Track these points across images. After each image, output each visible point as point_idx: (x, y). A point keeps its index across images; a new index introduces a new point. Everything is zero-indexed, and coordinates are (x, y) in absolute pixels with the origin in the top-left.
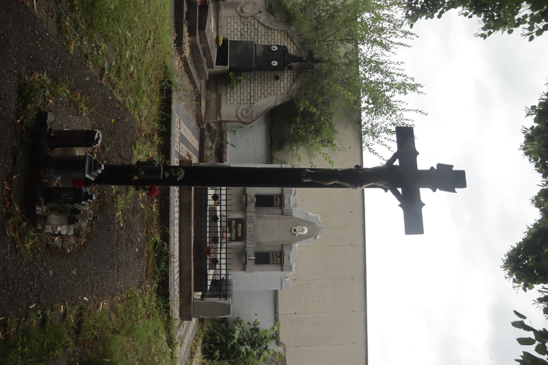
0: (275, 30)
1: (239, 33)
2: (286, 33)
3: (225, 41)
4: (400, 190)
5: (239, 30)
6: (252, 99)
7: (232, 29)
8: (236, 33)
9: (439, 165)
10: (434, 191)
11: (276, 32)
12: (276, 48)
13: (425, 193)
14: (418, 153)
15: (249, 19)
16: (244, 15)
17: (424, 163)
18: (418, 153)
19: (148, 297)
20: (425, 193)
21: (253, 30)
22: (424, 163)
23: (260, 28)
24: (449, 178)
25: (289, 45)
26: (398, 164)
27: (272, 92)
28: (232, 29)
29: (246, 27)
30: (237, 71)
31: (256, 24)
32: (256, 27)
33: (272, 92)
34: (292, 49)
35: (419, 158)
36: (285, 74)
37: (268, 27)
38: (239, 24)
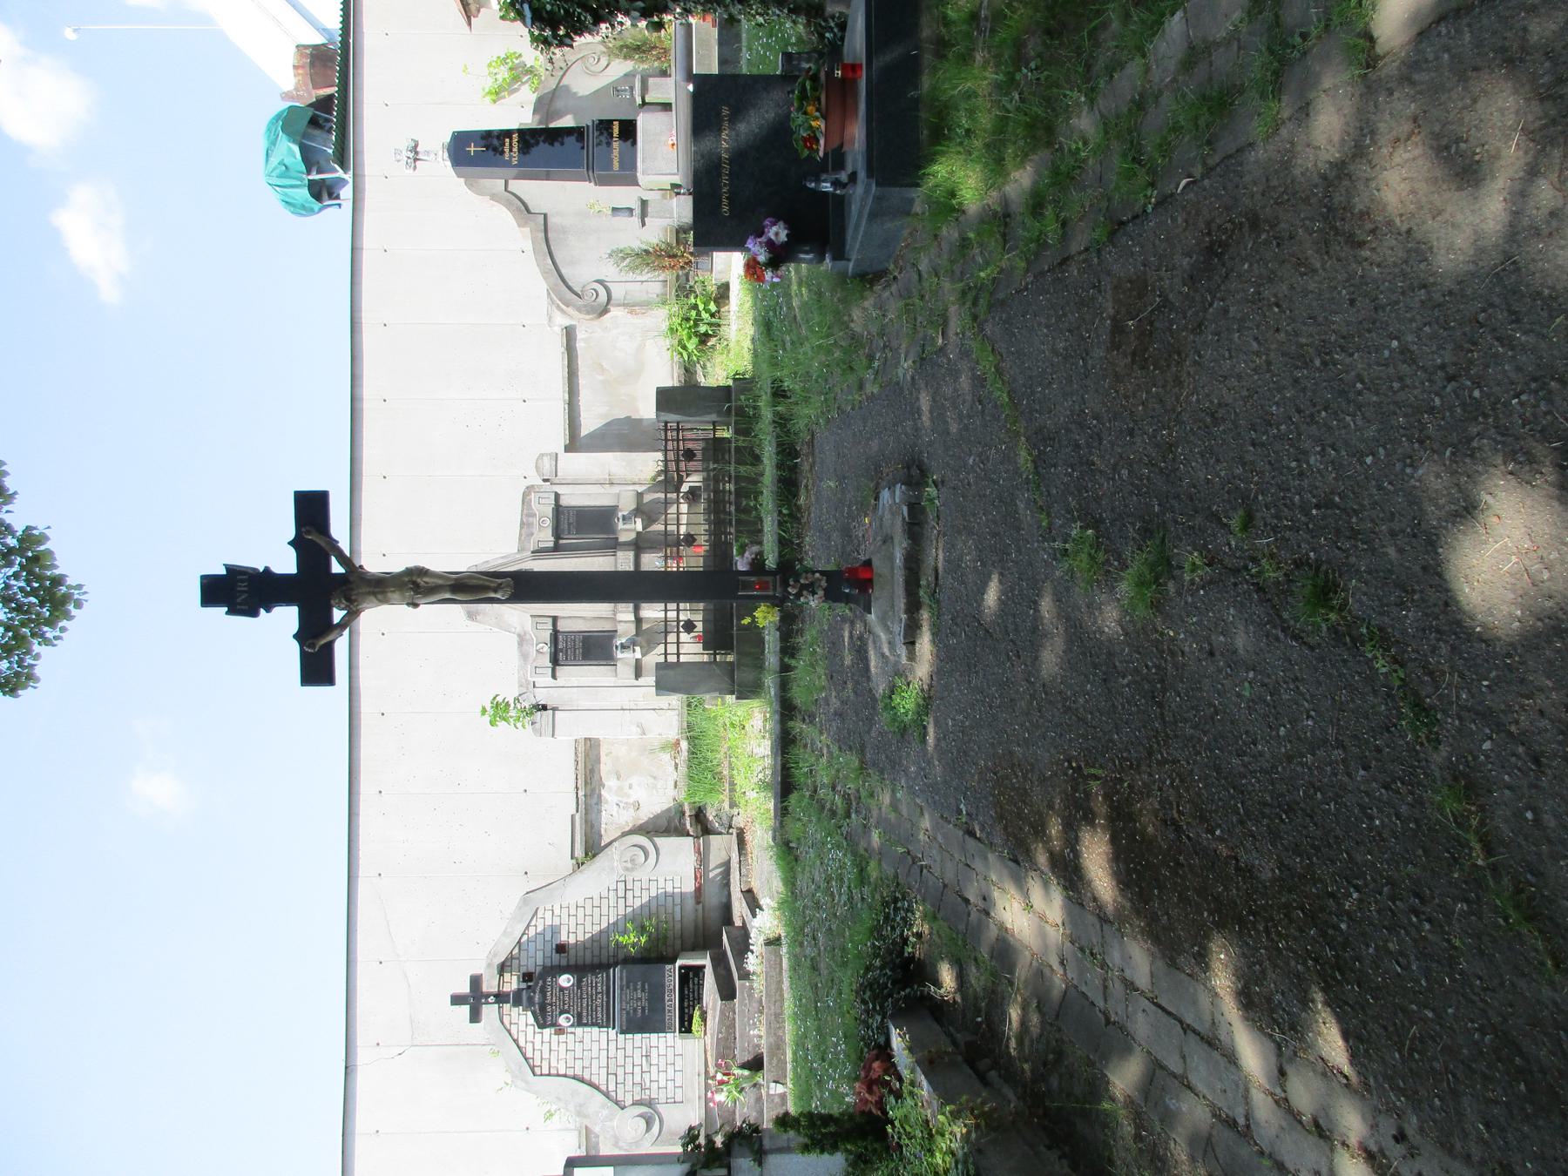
0: (565, 1076)
1: (654, 1061)
2: (538, 1071)
3: (686, 1027)
4: (337, 568)
5: (654, 1069)
6: (621, 894)
7: (670, 1069)
8: (662, 1059)
9: (254, 614)
10: (267, 570)
11: (562, 1072)
12: (562, 1020)
13: (285, 563)
14: (295, 636)
15: (629, 1102)
16: (644, 1109)
17: (286, 618)
18: (295, 636)
19: (806, 415)
20: (285, 563)
21: (620, 1071)
22: (286, 618)
23: (600, 1079)
24: (236, 591)
25: (530, 1038)
26: (335, 610)
27: (573, 912)
28: (670, 1069)
29: (638, 1079)
30: (655, 955)
31: (612, 1087)
32: (612, 1077)
33: (573, 912)
34: (522, 1027)
35: (295, 627)
36: (540, 962)
37: (582, 1080)
38: (654, 1085)
